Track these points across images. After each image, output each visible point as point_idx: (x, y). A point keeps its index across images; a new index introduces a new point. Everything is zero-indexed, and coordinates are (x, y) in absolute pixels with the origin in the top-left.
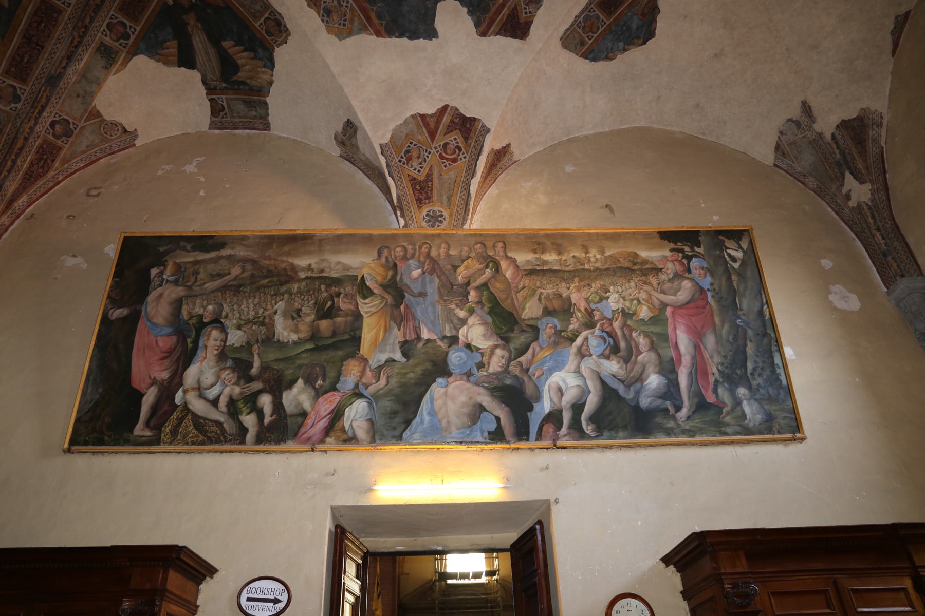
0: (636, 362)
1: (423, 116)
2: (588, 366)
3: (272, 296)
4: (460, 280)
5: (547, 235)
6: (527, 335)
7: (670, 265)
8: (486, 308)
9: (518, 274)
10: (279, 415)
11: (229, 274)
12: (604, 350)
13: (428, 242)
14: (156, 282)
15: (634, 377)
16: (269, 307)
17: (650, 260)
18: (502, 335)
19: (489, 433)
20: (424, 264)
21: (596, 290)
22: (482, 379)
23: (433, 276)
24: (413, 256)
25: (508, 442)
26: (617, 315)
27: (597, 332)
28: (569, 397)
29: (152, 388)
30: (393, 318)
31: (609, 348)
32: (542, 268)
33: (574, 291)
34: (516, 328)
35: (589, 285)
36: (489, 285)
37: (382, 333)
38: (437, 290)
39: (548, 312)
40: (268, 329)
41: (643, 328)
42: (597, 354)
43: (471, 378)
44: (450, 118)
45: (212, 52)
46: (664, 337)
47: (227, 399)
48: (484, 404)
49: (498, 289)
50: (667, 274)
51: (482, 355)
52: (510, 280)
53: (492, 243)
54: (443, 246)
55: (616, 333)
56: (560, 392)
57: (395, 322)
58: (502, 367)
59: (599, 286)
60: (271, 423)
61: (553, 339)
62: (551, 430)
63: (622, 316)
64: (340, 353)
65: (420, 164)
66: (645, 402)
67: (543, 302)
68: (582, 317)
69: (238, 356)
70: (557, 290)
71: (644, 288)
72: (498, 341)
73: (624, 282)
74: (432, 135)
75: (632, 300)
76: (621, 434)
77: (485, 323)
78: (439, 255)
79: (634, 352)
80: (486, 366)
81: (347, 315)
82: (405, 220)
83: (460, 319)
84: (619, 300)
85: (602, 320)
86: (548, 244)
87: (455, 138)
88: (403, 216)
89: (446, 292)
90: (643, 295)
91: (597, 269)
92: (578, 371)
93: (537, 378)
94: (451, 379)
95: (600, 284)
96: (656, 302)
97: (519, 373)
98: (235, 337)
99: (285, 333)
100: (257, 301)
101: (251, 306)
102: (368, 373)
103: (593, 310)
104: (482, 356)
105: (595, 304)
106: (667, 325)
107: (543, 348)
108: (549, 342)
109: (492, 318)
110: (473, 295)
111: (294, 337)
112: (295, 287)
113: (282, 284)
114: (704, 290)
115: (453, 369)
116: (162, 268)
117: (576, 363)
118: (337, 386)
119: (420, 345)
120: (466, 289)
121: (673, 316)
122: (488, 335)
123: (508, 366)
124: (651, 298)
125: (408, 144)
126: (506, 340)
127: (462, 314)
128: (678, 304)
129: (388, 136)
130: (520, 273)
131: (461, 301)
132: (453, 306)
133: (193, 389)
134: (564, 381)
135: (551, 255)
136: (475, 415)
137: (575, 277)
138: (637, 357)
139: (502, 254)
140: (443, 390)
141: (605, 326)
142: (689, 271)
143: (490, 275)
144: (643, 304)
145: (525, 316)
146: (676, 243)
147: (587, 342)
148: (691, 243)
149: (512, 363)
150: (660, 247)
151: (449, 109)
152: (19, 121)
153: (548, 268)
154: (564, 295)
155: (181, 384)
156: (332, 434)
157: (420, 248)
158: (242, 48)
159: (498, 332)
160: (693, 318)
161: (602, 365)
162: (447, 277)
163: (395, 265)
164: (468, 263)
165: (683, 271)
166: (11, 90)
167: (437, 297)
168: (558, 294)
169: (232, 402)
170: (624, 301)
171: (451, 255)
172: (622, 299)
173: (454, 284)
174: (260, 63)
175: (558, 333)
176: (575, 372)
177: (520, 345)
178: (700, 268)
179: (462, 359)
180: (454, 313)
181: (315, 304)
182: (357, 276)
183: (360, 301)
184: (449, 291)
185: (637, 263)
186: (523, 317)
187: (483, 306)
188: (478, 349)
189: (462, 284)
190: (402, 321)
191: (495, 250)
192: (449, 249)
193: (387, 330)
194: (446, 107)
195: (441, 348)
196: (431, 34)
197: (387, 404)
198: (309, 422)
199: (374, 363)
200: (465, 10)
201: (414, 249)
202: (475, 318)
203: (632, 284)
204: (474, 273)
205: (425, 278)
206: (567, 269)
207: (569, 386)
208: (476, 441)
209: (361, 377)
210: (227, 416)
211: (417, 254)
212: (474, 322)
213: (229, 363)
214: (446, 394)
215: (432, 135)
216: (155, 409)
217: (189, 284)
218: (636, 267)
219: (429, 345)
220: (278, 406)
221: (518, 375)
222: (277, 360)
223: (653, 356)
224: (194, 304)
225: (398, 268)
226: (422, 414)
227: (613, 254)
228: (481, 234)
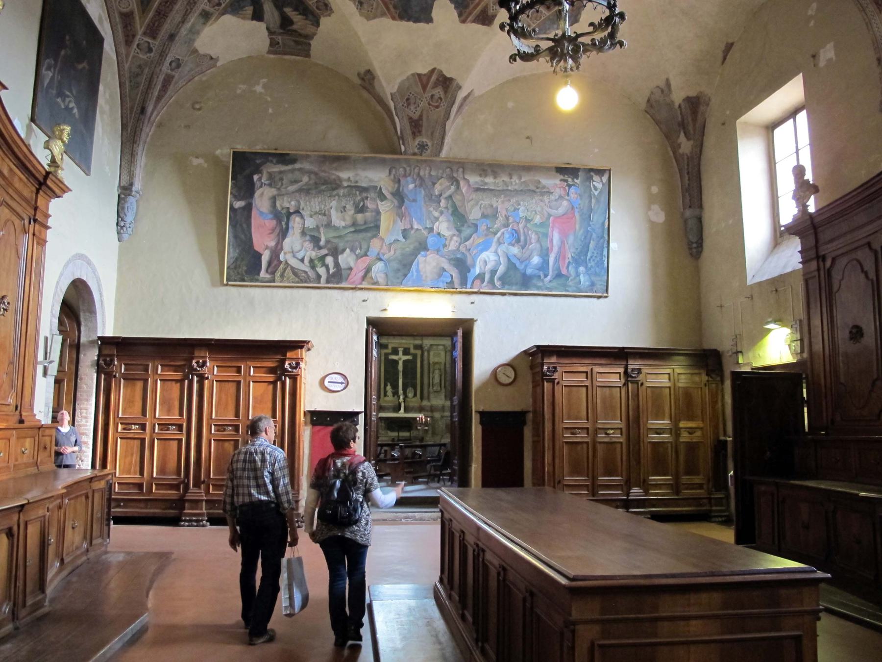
0: (528, 248)
1: (419, 75)
3: (328, 197)
4: (437, 192)
7: (558, 190)
10: (337, 269)
11: (301, 181)
14: (258, 184)
16: (327, 204)
24: (409, 175)
27: (510, 229)
28: (490, 266)
29: (267, 251)
30: (398, 215)
34: (466, 225)
35: (509, 200)
37: (392, 223)
39: (484, 216)
40: (327, 218)
41: (537, 229)
44: (436, 77)
45: (276, 14)
46: (546, 235)
47: (309, 259)
48: (445, 267)
56: (485, 262)
57: (399, 217)
60: (334, 274)
61: (485, 232)
64: (369, 235)
65: (416, 108)
66: (529, 271)
69: (312, 234)
74: (424, 88)
75: (532, 211)
76: (514, 288)
77: (448, 221)
78: (425, 175)
81: (372, 211)
82: (404, 146)
83: (435, 217)
87: (439, 92)
88: (404, 144)
90: (539, 209)
91: (515, 190)
92: (496, 252)
94: (428, 253)
98: (310, 223)
99: (338, 221)
100: (320, 199)
101: (317, 204)
102: (384, 247)
110: (443, 203)
111: (343, 224)
112: (341, 192)
113: (334, 189)
116: (260, 175)
117: (495, 247)
118: (368, 254)
119: (413, 232)
121: (553, 224)
123: (459, 247)
125: (409, 94)
126: (459, 231)
127: (436, 214)
129: (396, 87)
132: (431, 209)
133: (289, 252)
134: (489, 258)
138: (529, 246)
139: (461, 176)
141: (515, 226)
142: (568, 195)
146: (564, 176)
151: (436, 71)
152: (153, 66)
154: (494, 206)
155: (282, 249)
156: (366, 280)
157: (414, 169)
158: (297, 13)
163: (399, 181)
166: (146, 45)
169: (311, 261)
174: (308, 22)
175: (488, 229)
181: (354, 203)
182: (377, 187)
183: (379, 202)
190: (403, 216)
192: (431, 170)
193: (395, 222)
194: (433, 70)
196: (429, 20)
197: (395, 265)
198: (353, 273)
199: (387, 241)
200: (453, 6)
201: (410, 170)
203: (534, 201)
206: (498, 189)
209: (381, 249)
210: (309, 268)
211: (412, 174)
213: (308, 238)
214: (425, 261)
215: (424, 88)
216: (270, 263)
217: (278, 187)
218: (538, 190)
220: (337, 264)
222: (335, 237)
223: (538, 245)
224: (283, 200)
225: (401, 183)
226: (412, 272)
228: (450, 162)
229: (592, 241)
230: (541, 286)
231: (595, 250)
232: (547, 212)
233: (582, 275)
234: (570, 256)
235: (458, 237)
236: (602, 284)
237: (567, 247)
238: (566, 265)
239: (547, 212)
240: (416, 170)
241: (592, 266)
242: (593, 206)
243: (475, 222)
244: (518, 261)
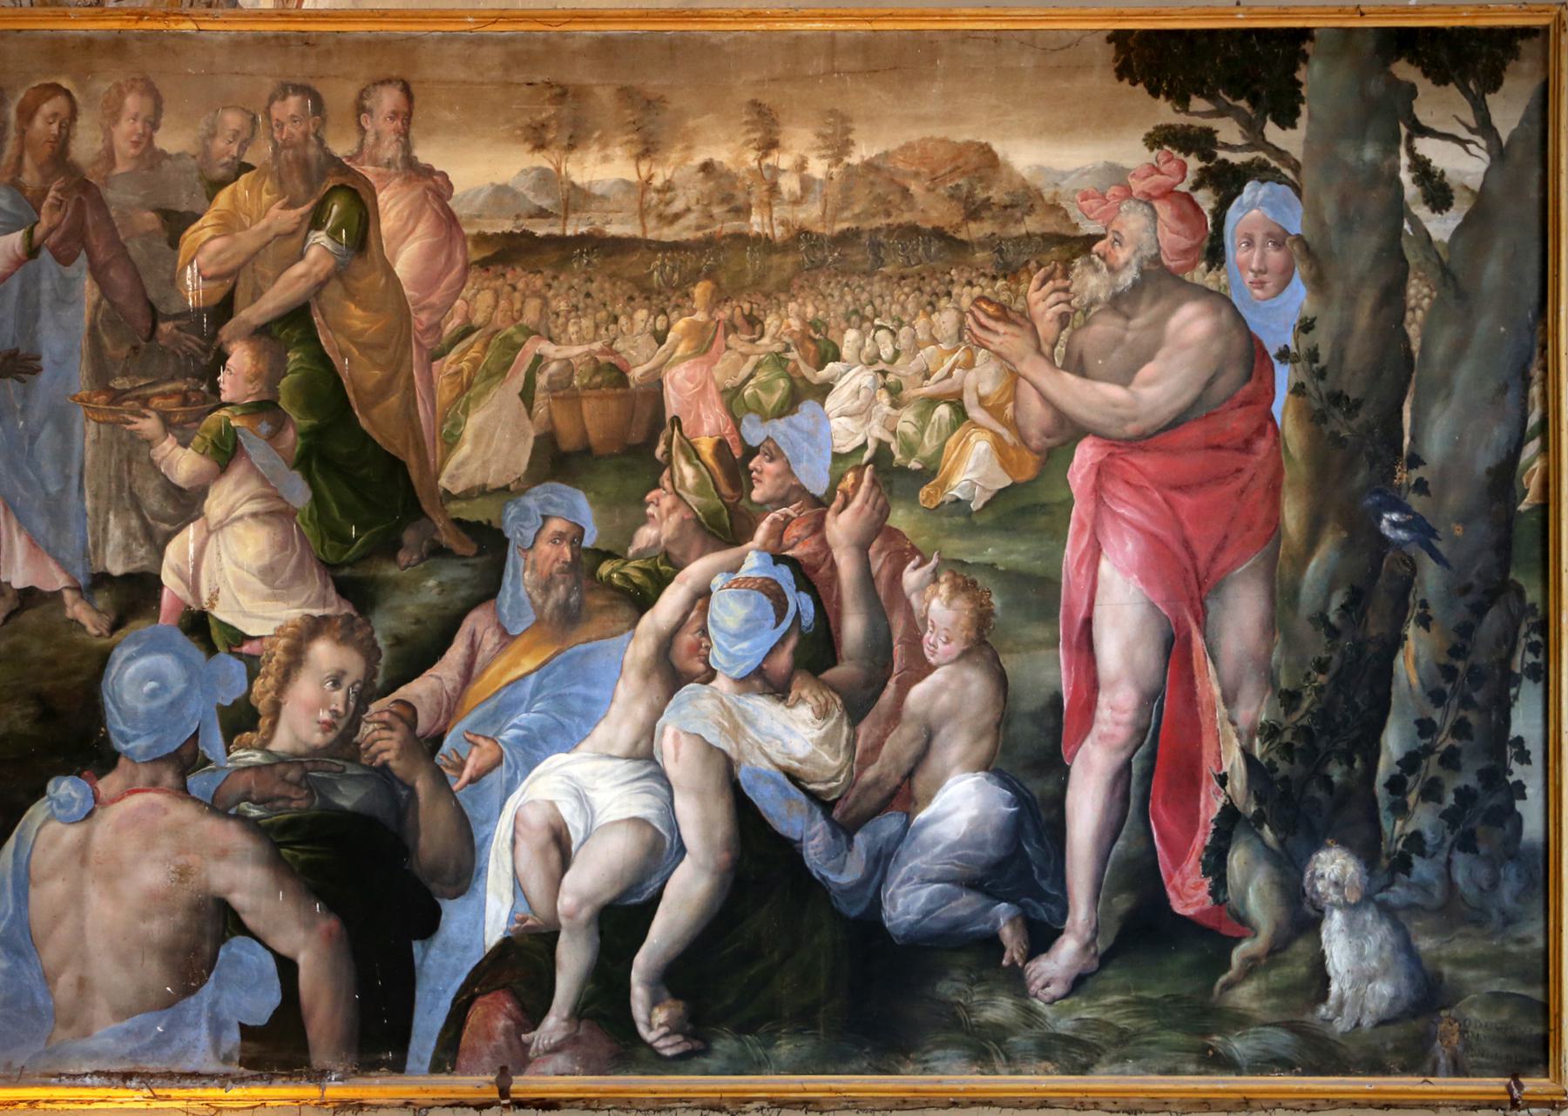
0: (896, 715)
2: (692, 729)
4: (193, 288)
5: (606, 49)
6: (451, 572)
7: (1133, 221)
8: (290, 436)
9: (450, 257)
12: (773, 651)
13: (65, 83)
15: (877, 782)
17: (1048, 194)
18: (346, 572)
19: (247, 1032)
20: (36, 204)
21: (777, 347)
22: (239, 785)
23: (71, 271)
25: (319, 1076)
26: (850, 477)
27: (753, 561)
31: (791, 643)
32: (557, 231)
33: (678, 353)
34: (409, 536)
35: (753, 323)
36: (317, 319)
38: (84, 344)
41: (955, 547)
42: (740, 670)
43: (196, 782)
48: (238, 900)
49: (353, 337)
50: (1111, 269)
51: (253, 667)
52: (408, 292)
53: (351, 91)
54: (132, 102)
55: (833, 566)
58: (328, 726)
59: (795, 324)
61: (559, 592)
62: (501, 1023)
63: (874, 482)
67: (541, 410)
68: (700, 489)
70: (609, 349)
71: (996, 342)
72: (324, 602)
73: (910, 307)
75: (932, 401)
77: (277, 513)
78: (109, 156)
79: (895, 670)
80: (264, 723)
84: (873, 399)
85: (784, 502)
86: (605, 95)
89: (125, 350)
90: (983, 380)
91: (802, 235)
92: (644, 754)
93: (472, 781)
94: (110, 784)
95: (802, 317)
96: (1035, 414)
97: (398, 758)
103: (751, 452)
104: (252, 675)
105: (765, 418)
106: (1061, 537)
107: (514, 638)
108: (539, 610)
109: (312, 484)
114: (1265, 353)
115: (121, 735)
117: (641, 711)
120: (215, 336)
121: (1098, 492)
122: (288, 573)
123: (354, 723)
124: (1014, 397)
127: (183, 463)
128: (1131, 429)
130: (459, 256)
131: (185, 401)
132: (149, 425)
134: (581, 798)
135: (606, 159)
136: (194, 949)
137: (694, 277)
138: (903, 690)
140: (71, 834)
141: (794, 531)
142: (1215, 254)
143: (327, 264)
144: (976, 425)
145: (452, 477)
146: (1182, 102)
147: (705, 610)
148: (1254, 102)
149: (373, 707)
150: (1107, 121)
153: (583, 229)
154: (636, 374)
157: (27, 114)
159: (332, 559)
160: (1185, 502)
161: (752, 724)
162: (137, 277)
164: (234, 193)
165: (1185, 252)
167: (80, 379)
168: (612, 367)
170: (895, 405)
171: (164, 155)
172: (884, 398)
173: (162, 309)
176: (629, 757)
177: (418, 621)
178: (1269, 235)
179: (164, 687)
180: (151, 461)
184: (135, 348)
185: (987, 204)
186: (443, 482)
187: (279, 422)
188: (237, 638)
189: (197, 310)
191: (362, 131)
192: (154, 124)
195: (78, 636)
202: (238, 484)
203: (946, 320)
204: (255, 255)
205: (37, 281)
206: (669, 234)
207: (602, 820)
208: (189, 1067)
212: (232, 509)
214: (82, 852)
218: (977, 230)
219: (31, 617)
221: (393, 764)
223: (976, 683)
227: (886, 155)
229: (1412, 630)
230: (999, 1033)
231: (1437, 698)
232: (1046, 399)
233: (1335, 922)
234: (1233, 761)
235: (343, 641)
236: (1498, 998)
237: (1210, 686)
238: (1203, 838)
239: (1046, 399)
240: (43, 125)
241: (1416, 839)
242: (1413, 331)
243: (474, 512)
244: (820, 825)
